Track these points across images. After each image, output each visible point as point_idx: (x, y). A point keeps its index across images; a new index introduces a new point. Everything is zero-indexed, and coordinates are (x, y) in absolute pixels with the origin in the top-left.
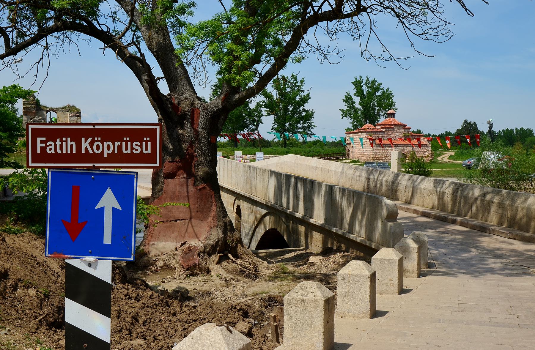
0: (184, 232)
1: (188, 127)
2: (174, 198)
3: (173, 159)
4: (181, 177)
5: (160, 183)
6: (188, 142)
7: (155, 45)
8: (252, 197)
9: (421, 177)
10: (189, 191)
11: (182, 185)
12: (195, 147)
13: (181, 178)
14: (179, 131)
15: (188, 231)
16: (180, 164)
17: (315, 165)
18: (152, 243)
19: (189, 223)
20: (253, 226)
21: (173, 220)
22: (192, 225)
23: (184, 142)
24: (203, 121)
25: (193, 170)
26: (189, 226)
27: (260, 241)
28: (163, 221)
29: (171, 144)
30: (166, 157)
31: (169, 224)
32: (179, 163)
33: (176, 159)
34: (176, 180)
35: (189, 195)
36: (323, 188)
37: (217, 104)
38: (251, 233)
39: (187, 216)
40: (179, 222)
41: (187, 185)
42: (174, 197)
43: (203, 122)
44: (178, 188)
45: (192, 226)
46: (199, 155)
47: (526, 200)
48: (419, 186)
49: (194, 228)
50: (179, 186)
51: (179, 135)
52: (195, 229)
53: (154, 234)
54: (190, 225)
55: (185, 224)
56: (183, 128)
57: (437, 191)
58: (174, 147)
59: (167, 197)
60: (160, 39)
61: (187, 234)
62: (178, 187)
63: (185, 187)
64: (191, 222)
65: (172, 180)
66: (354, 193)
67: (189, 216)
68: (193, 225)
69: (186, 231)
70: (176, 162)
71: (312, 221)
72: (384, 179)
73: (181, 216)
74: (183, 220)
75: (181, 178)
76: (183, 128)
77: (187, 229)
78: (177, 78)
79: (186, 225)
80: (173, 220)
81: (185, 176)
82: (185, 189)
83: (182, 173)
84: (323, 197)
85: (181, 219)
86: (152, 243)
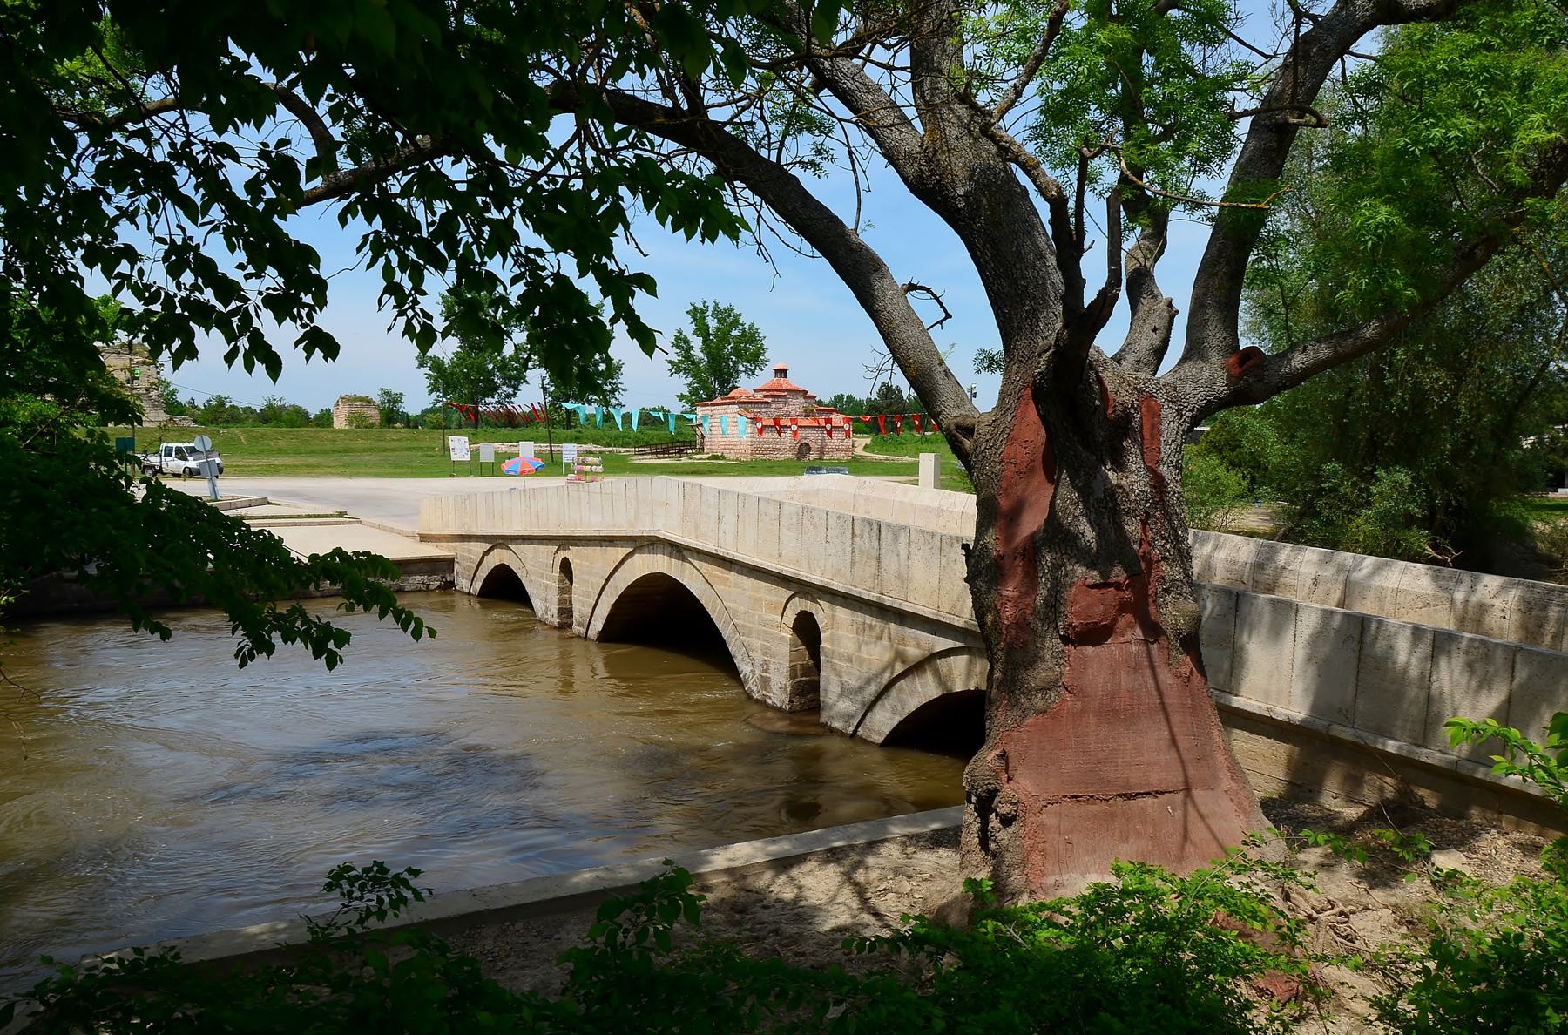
0: (1178, 838)
1: (1135, 462)
2: (1115, 713)
3: (1105, 574)
4: (1128, 637)
5: (1042, 659)
6: (1139, 515)
7: (962, 175)
8: (892, 601)
9: (1370, 560)
10: (1163, 687)
11: (1136, 669)
12: (1151, 530)
13: (1128, 641)
14: (1110, 474)
15: (1194, 836)
16: (1128, 594)
17: (936, 505)
18: (1051, 880)
19: (1185, 804)
20: (883, 671)
21: (1120, 795)
22: (1198, 811)
23: (1127, 513)
24: (1173, 441)
25: (1152, 608)
26: (1189, 818)
27: (913, 715)
28: (1076, 797)
29: (1090, 523)
30: (1069, 568)
31: (1097, 807)
32: (1123, 591)
33: (1117, 576)
34: (1111, 649)
35: (1166, 701)
36: (1430, 636)
37: (1210, 383)
38: (872, 689)
39: (1177, 780)
40: (1149, 800)
41: (1152, 667)
42: (1116, 712)
43: (1173, 445)
44: (1125, 679)
45: (1202, 816)
46: (1165, 559)
47: (1473, 589)
48: (1373, 582)
49: (1210, 822)
50: (1128, 673)
51: (1112, 492)
52: (1215, 828)
53: (1047, 845)
54: (1190, 808)
55: (1173, 810)
56: (1120, 466)
57: (1452, 601)
58: (1100, 535)
59: (1083, 711)
60: (984, 154)
61: (1189, 848)
62: (1124, 674)
63: (1148, 672)
64: (1193, 802)
65: (1098, 649)
66: (1518, 658)
67: (1181, 779)
68: (1204, 810)
69: (1186, 836)
70: (1118, 586)
71: (1239, 702)
72: (1221, 555)
73: (1155, 779)
74: (1161, 793)
75: (1128, 641)
76: (1120, 466)
77: (1186, 829)
78: (1045, 290)
79: (1179, 812)
80: (1120, 795)
81: (1139, 632)
82: (1151, 683)
83: (1130, 626)
84: (1301, 642)
85: (1157, 792)
86: (1051, 880)
